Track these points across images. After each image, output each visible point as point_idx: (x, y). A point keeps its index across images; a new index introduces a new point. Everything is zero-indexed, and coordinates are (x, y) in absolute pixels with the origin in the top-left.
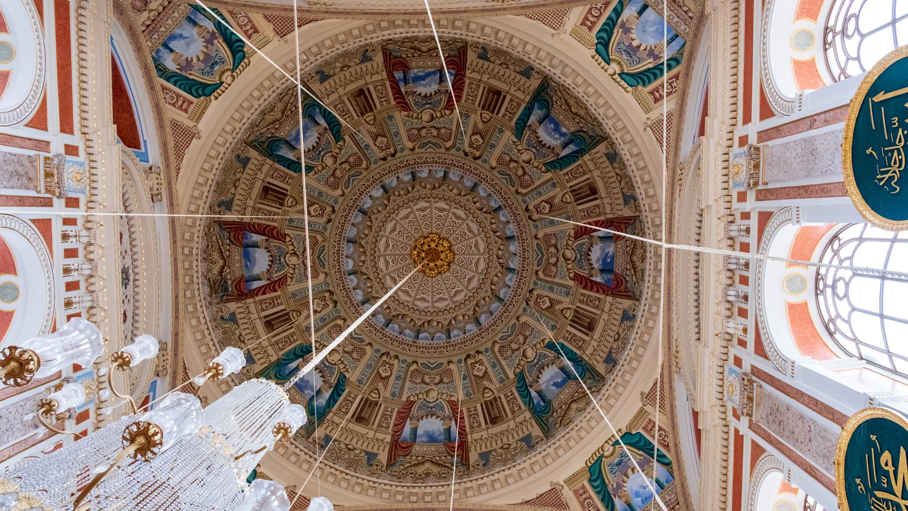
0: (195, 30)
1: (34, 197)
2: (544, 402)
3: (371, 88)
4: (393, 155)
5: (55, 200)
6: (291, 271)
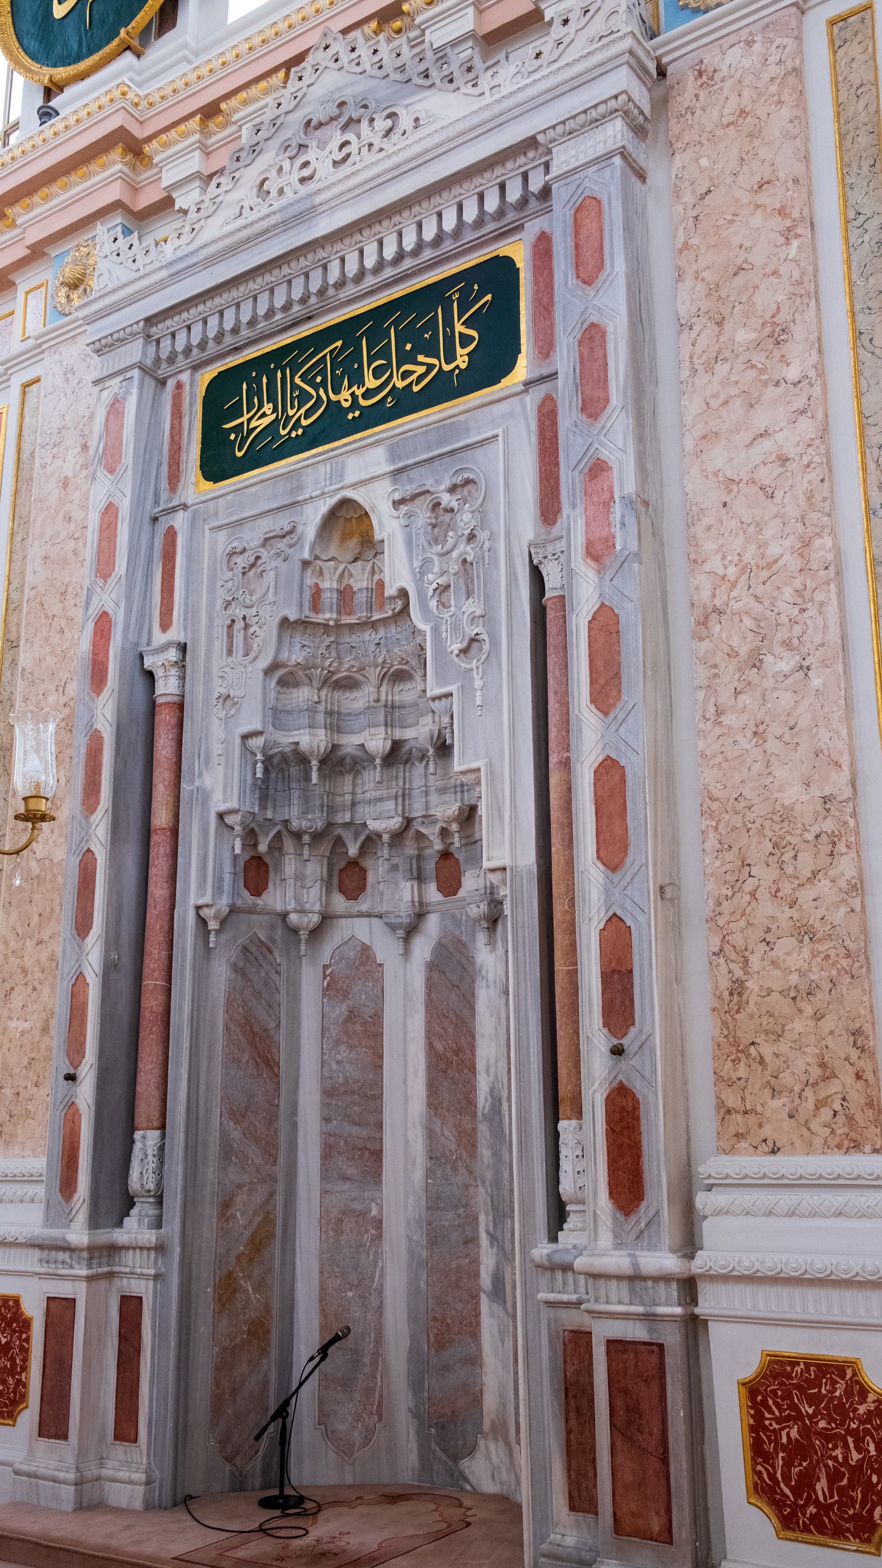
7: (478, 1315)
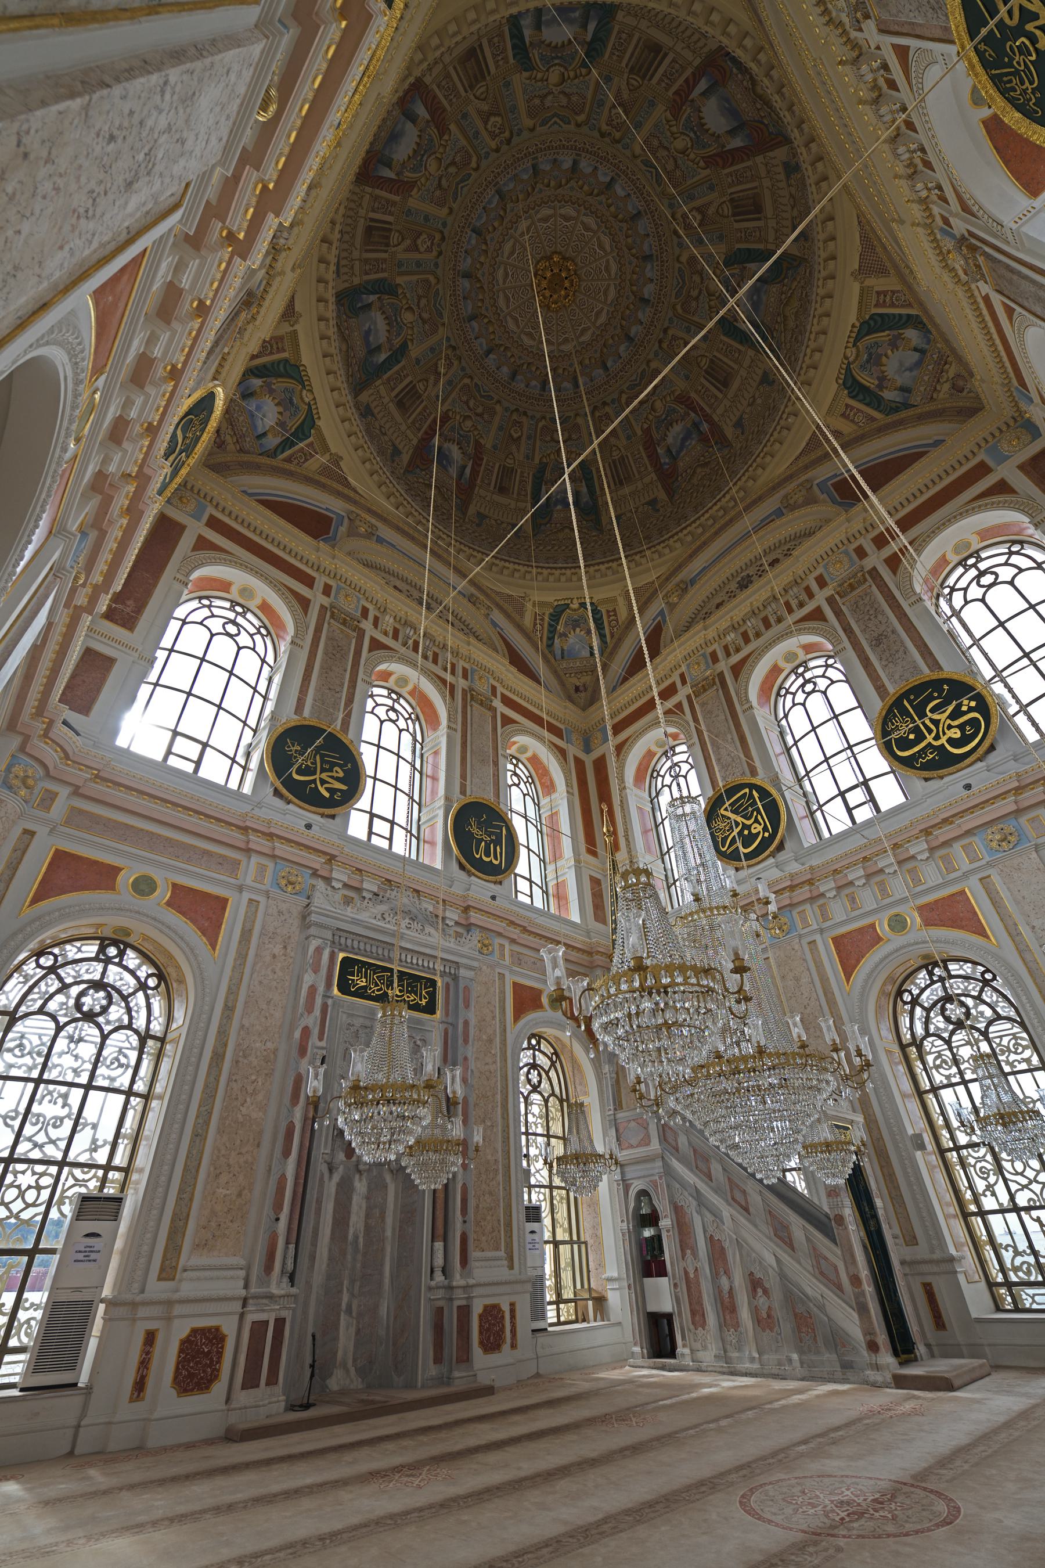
0: (899, 384)
2: (361, 308)
3: (720, 395)
4: (660, 342)
6: (674, 129)
7: (339, 1320)
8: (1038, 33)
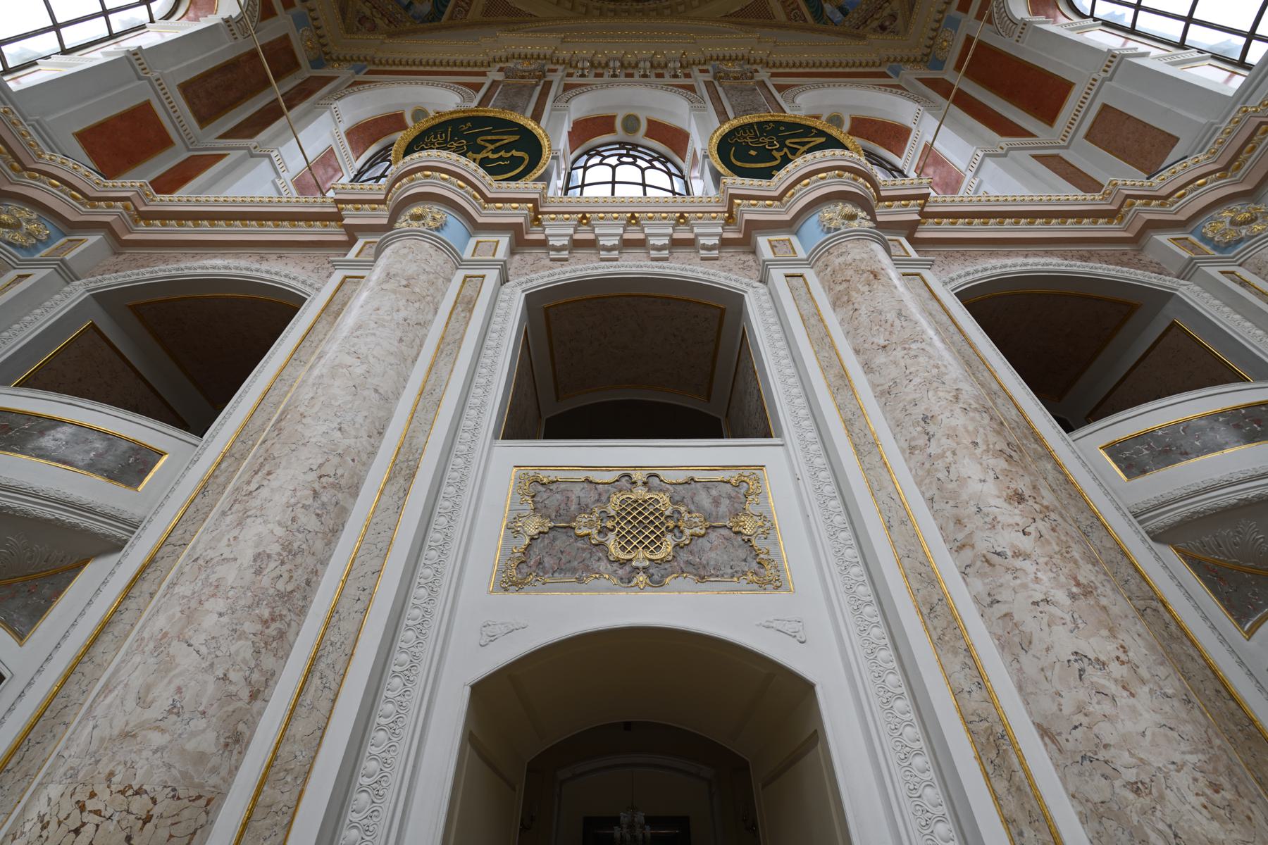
1: (543, 88)
5: (548, 79)
8: (782, 153)
